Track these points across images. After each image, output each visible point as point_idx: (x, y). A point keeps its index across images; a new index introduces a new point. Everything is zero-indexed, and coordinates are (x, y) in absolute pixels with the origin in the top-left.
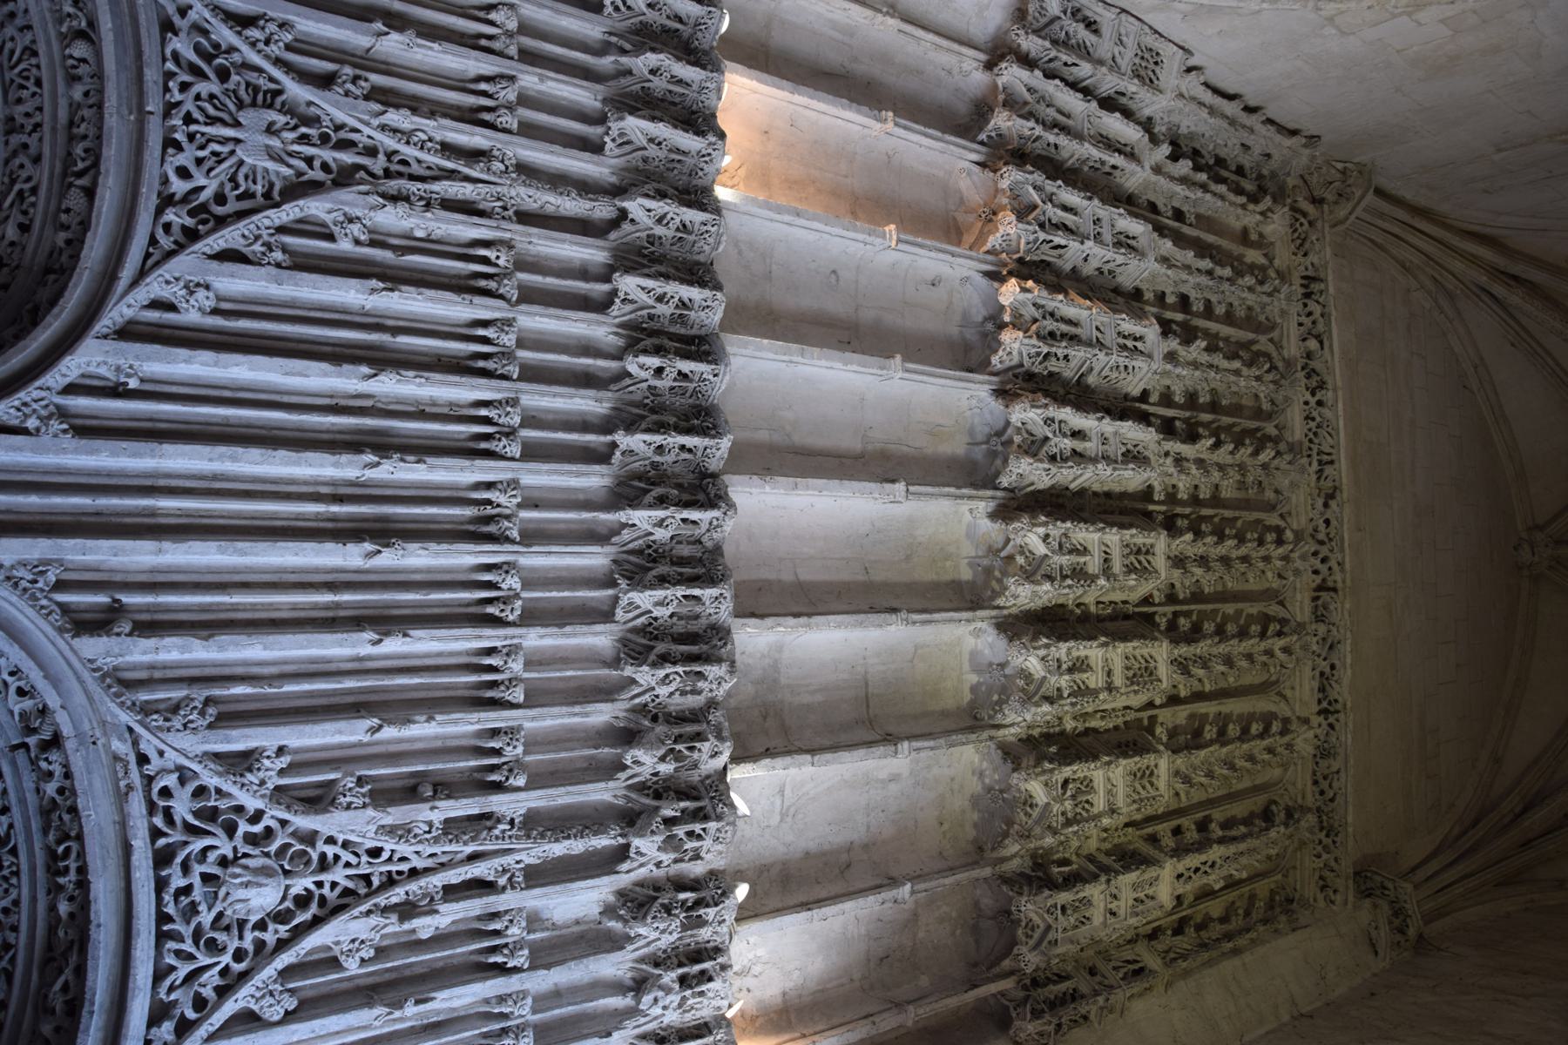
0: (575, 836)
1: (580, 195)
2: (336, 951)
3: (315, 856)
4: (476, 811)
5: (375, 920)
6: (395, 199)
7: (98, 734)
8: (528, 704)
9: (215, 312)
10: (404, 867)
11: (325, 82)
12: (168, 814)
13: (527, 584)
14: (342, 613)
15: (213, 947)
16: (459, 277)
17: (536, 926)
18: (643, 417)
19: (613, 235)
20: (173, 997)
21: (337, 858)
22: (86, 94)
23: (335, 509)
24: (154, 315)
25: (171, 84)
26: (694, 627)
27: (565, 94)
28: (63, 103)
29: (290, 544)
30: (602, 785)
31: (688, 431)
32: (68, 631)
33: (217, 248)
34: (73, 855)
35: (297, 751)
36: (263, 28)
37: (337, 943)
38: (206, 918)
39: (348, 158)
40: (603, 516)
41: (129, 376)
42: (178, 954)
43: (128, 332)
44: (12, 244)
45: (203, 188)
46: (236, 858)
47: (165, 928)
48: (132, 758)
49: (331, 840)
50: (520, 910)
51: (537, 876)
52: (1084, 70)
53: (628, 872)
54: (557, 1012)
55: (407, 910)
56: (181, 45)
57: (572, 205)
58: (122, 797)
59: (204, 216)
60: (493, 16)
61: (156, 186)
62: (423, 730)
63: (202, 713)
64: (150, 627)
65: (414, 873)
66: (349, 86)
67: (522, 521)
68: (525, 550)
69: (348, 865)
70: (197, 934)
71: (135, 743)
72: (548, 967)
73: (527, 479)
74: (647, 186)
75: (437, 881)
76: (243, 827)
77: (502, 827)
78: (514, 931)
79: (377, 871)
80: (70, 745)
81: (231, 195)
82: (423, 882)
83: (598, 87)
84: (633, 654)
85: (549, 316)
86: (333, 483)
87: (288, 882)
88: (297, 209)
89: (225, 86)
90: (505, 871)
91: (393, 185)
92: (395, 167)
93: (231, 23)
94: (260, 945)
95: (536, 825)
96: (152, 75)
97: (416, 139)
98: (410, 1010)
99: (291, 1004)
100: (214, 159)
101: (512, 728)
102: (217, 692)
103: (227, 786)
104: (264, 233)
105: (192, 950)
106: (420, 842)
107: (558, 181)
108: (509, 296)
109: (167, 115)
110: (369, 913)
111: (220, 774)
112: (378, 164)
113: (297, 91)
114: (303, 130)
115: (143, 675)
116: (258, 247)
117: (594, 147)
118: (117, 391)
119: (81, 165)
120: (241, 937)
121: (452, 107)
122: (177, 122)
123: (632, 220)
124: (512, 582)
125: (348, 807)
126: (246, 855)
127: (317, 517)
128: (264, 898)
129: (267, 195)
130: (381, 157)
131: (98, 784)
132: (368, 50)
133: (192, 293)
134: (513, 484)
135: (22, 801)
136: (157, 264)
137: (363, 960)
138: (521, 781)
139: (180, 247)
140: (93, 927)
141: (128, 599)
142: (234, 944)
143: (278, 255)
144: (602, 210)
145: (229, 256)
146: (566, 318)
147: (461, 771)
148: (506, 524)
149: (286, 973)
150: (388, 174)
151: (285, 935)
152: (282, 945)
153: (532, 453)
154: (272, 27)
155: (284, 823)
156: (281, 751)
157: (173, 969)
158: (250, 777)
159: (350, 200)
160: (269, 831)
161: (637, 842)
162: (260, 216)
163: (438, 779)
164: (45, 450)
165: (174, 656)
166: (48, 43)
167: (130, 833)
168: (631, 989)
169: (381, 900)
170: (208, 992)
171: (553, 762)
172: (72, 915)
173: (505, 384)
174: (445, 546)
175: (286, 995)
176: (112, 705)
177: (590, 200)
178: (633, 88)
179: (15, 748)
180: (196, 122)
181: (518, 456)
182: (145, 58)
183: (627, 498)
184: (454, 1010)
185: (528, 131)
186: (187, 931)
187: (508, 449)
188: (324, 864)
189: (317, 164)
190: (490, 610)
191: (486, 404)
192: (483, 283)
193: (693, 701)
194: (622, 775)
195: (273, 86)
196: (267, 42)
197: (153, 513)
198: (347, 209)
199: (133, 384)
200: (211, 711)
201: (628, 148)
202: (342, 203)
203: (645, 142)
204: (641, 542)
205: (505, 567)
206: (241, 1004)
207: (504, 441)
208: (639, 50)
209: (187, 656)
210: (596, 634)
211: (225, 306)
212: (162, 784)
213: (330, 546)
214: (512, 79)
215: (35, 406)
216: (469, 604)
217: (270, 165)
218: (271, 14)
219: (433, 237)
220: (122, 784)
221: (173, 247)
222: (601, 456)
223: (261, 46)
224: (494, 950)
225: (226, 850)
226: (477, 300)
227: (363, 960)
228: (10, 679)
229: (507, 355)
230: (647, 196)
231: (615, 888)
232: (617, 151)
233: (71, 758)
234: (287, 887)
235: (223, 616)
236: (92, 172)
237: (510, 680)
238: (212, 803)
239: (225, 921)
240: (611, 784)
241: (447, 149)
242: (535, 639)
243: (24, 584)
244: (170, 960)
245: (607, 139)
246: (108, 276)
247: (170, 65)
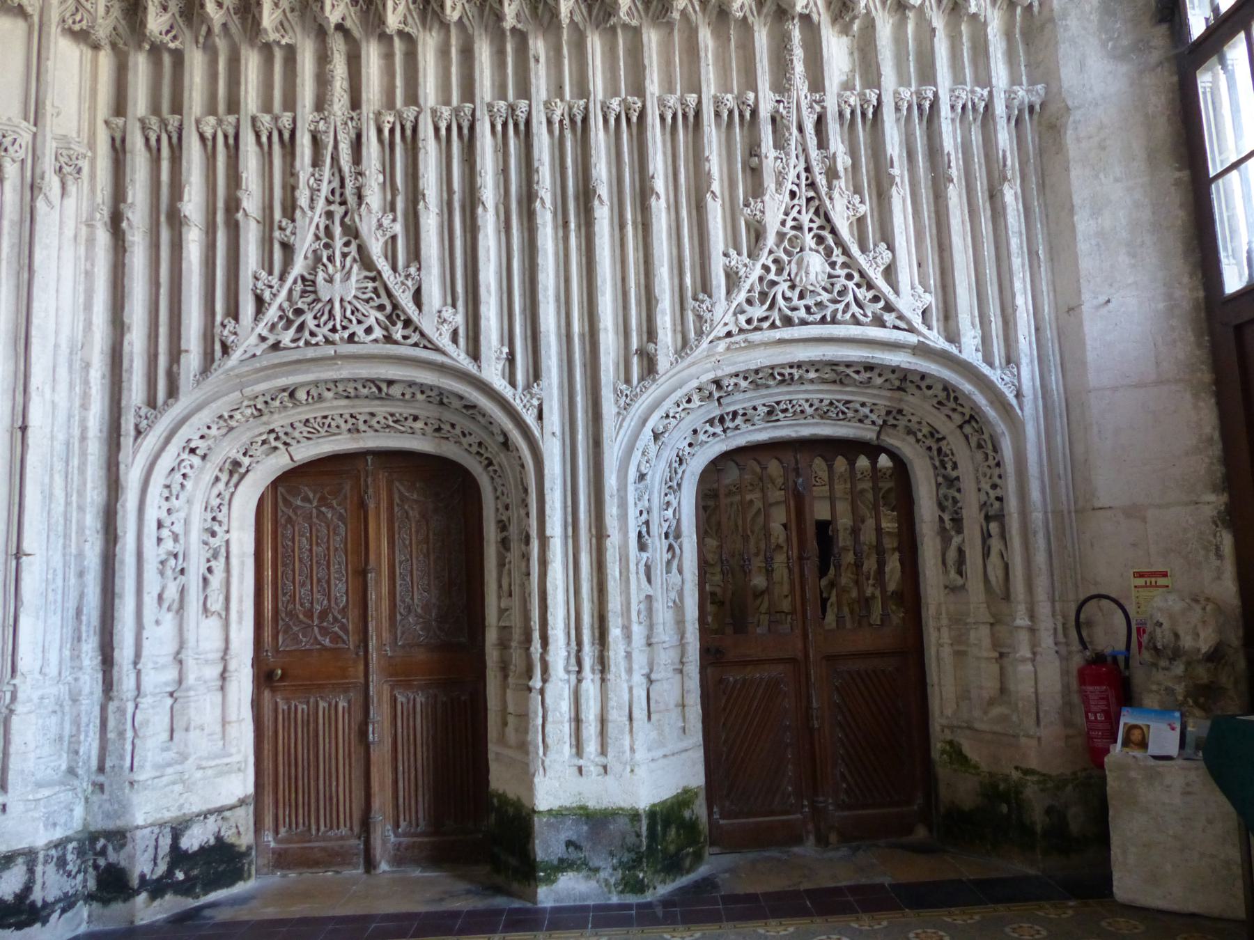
0: (791, 55)
1: (330, 62)
2: (853, 219)
3: (793, 232)
4: (770, 127)
5: (836, 194)
6: (360, 197)
7: (714, 359)
9: (454, 306)
10: (803, 175)
11: (287, 248)
12: (761, 320)
13: (616, 93)
14: (639, 219)
15: (842, 293)
16: (406, 150)
17: (850, 84)
18: (491, 6)
19: (357, 33)
20: (870, 314)
21: (794, 219)
22: (329, 390)
23: (572, 226)
24: (462, 341)
25: (313, 342)
27: (255, 76)
28: (336, 403)
29: (597, 253)
30: (756, 35)
32: (654, 377)
33: (414, 307)
34: (783, 371)
35: (726, 246)
36: (262, 290)
37: (848, 218)
38: (825, 297)
39: (337, 230)
40: (565, 37)
41: (501, 352)
42: (844, 312)
43: (475, 355)
44: (426, 424)
45: (377, 319)
46: (791, 280)
47: (829, 319)
48: (728, 340)
49: (783, 223)
50: (839, 96)
51: (817, 83)
53: (819, 15)
54: (912, 70)
55: (832, 174)
56: (287, 337)
57: (339, 69)
58: (751, 345)
59: (394, 317)
60: (209, 135)
61: (380, 345)
62: (715, 165)
63: (703, 302)
64: (651, 334)
65: (807, 169)
66: (288, 232)
67: (572, 98)
68: (592, 95)
69: (799, 212)
70: (835, 302)
71: (719, 338)
72: (879, 75)
73: (543, 95)
74: (314, 8)
75: (814, 153)
76: (772, 276)
77: (781, 109)
78: (852, 101)
79: (805, 193)
80: (720, 373)
81: (377, 302)
82: (814, 163)
83: (243, 52)
84: (663, 12)
85: (425, 82)
86: (555, 228)
87: (807, 249)
88: (380, 260)
89: (306, 310)
90: (811, 107)
91: (351, 199)
92: (337, 198)
93: (264, 310)
94: (844, 265)
95: (781, 84)
96: (311, 353)
97: (315, 185)
98: (896, 171)
99: (883, 246)
100: (356, 313)
101: (715, 102)
102: (689, 294)
103: (747, 286)
104: (399, 279)
105: (843, 304)
106: (788, 165)
107: (323, 81)
108: (415, 113)
109: (333, 343)
110: (831, 198)
111: (739, 291)
112: (338, 211)
113: (299, 267)
114: (325, 260)
115: (679, 337)
116: (409, 283)
117: (291, 54)
119: (374, 389)
120: (839, 277)
121: (284, 162)
122: (337, 337)
123: (343, 19)
124: (615, 103)
125: (763, 212)
126: (789, 275)
127: (578, 237)
128: (816, 264)
129: (374, 279)
130: (332, 208)
131: (742, 359)
132: (258, 222)
133: (445, 320)
134: (547, 105)
135: (750, 399)
136: (430, 341)
137: (861, 202)
138: (751, 95)
139: (416, 329)
140: (824, 359)
141: (635, 345)
142: (843, 281)
143: (412, 270)
144: (338, 47)
146: (425, 69)
147: (742, 137)
148: (575, 110)
149: (863, 249)
150: (343, 203)
151: (840, 250)
152: (846, 252)
153: (524, 91)
154: (260, 285)
155: (771, 252)
156: (726, 255)
157: (853, 315)
158: (741, 273)
159: (367, 227)
160: (776, 261)
161: (799, 8)
162: (388, 283)
163: (747, 153)
164: (551, 395)
165: (668, 319)
166: (300, 413)
167: (772, 340)
168: (904, 14)
169: (823, 190)
170: (870, 295)
171: (738, 71)
172: (817, 371)
173: (478, 114)
174: (593, 152)
175: (877, 249)
176: (697, 353)
177: (332, 53)
178: (237, 22)
179: (720, 403)
180: (334, 326)
181: (527, 102)
182: (301, 358)
183: (552, 17)
184: (901, 142)
185: (290, 103)
186: (832, 307)
187: (524, 109)
188: (798, 228)
189: (346, 250)
190: (634, 119)
191: (493, 126)
192: (409, 132)
194: (750, 19)
195: (299, 281)
196: (271, 287)
197: (582, 335)
198: (373, 229)
199: (506, 350)
200: (701, 296)
201: (286, 24)
202: (370, 230)
203: (280, 11)
204: (582, 6)
205: (605, 109)
206: (879, 276)
207: (518, 112)
208: (204, 18)
209: (668, 311)
210: (650, 41)
211: (449, 300)
212: (744, 323)
213: (597, 228)
214: (254, 119)
215: (525, 401)
216: (630, 135)
217: (354, 278)
218: (251, 286)
219: (381, 169)
220: (743, 345)
221: (417, 333)
222: (521, 38)
223: (274, 290)
224: (864, 114)
225: (784, 286)
226: (421, 135)
227: (861, 202)
228: (682, 407)
229: (457, 112)
230: (322, 8)
231: (830, 26)
232: (291, 33)
233: (727, 372)
234: (811, 249)
235: (643, 292)
236: (378, 383)
237: (682, 104)
238: (757, 295)
239: (829, 286)
240: (756, 28)
241: (316, 162)
242: (653, 87)
243: (628, 401)
244: (848, 316)
245: (283, 42)
246: (441, 368)
247: (301, 343)
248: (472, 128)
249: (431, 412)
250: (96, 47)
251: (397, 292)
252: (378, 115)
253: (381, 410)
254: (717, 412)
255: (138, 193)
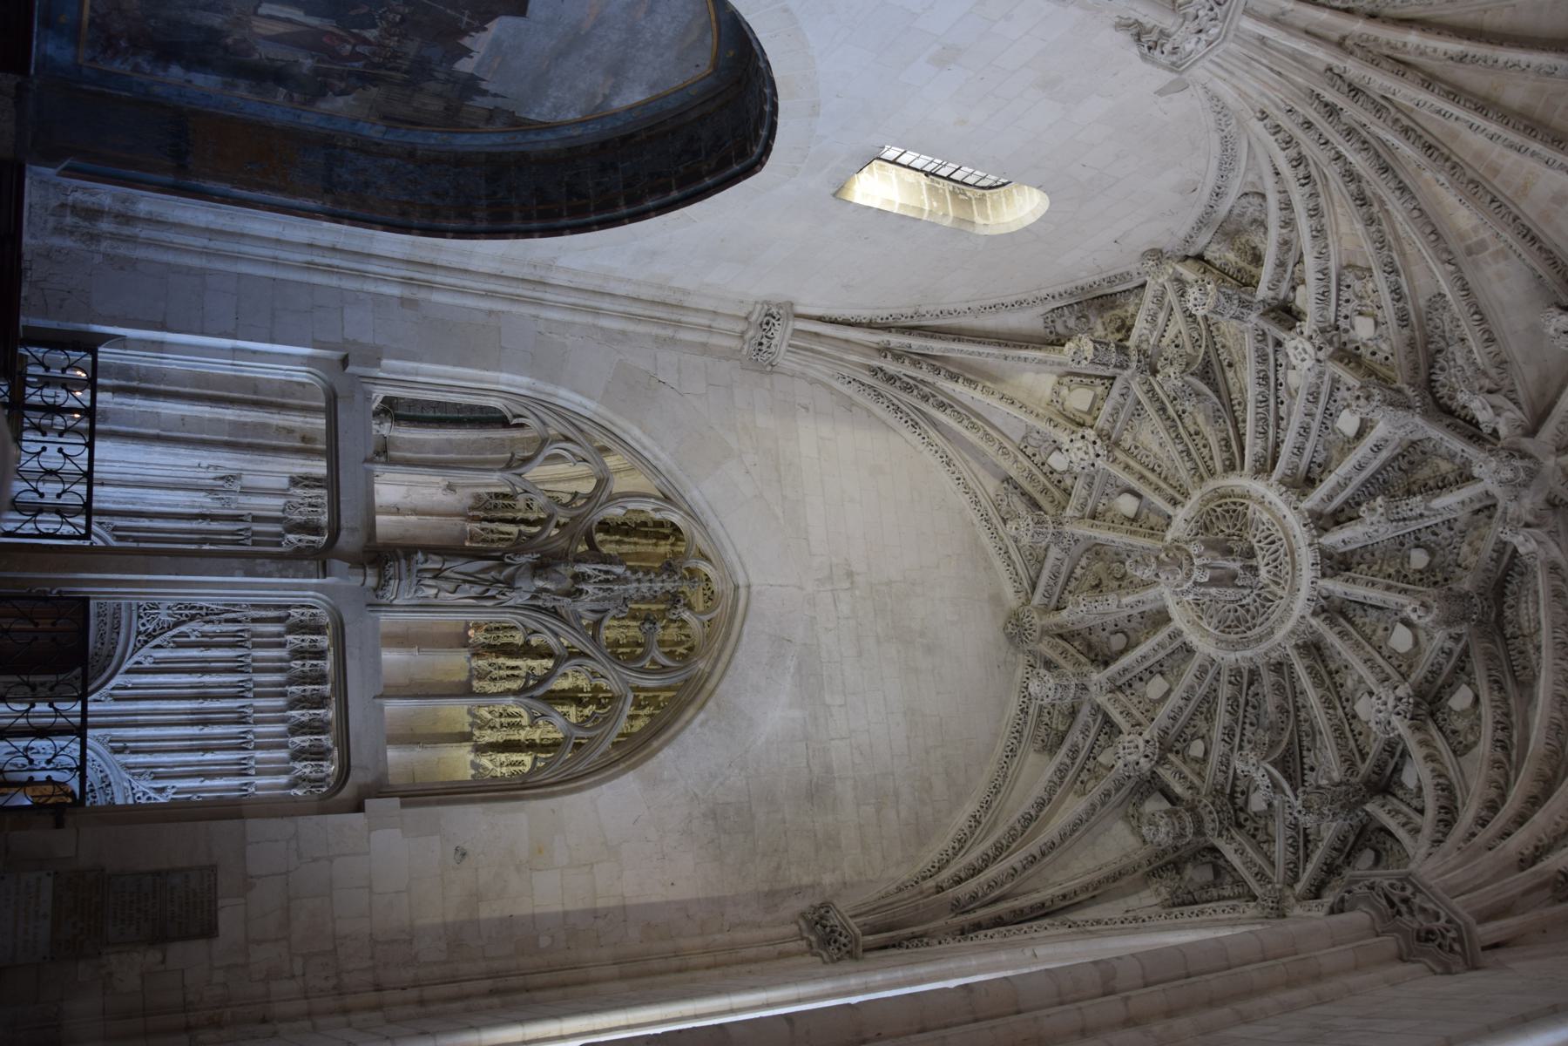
6: (212, 622)
8: (257, 774)
26: (322, 750)
31: (318, 684)
39: (194, 612)
43: (128, 672)
52: (509, 515)
62: (218, 782)
64: (135, 752)
73: (256, 704)
91: (208, 618)
112: (204, 611)
118: (126, 688)
124: (250, 736)
134: (251, 706)
145: (158, 647)
153: (257, 695)
159: (194, 625)
193: (320, 775)
222: (283, 694)
229: (248, 665)
242: (259, 754)
246: (123, 657)
248: (242, 672)
249: (105, 652)
250: (283, 511)
251: (162, 638)
252: (248, 630)
253: (107, 628)
254: (96, 787)
255: (215, 526)
